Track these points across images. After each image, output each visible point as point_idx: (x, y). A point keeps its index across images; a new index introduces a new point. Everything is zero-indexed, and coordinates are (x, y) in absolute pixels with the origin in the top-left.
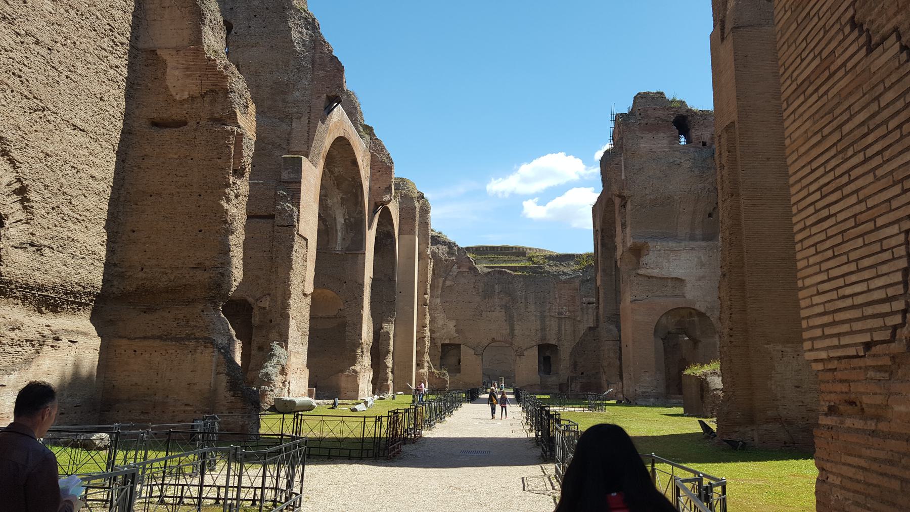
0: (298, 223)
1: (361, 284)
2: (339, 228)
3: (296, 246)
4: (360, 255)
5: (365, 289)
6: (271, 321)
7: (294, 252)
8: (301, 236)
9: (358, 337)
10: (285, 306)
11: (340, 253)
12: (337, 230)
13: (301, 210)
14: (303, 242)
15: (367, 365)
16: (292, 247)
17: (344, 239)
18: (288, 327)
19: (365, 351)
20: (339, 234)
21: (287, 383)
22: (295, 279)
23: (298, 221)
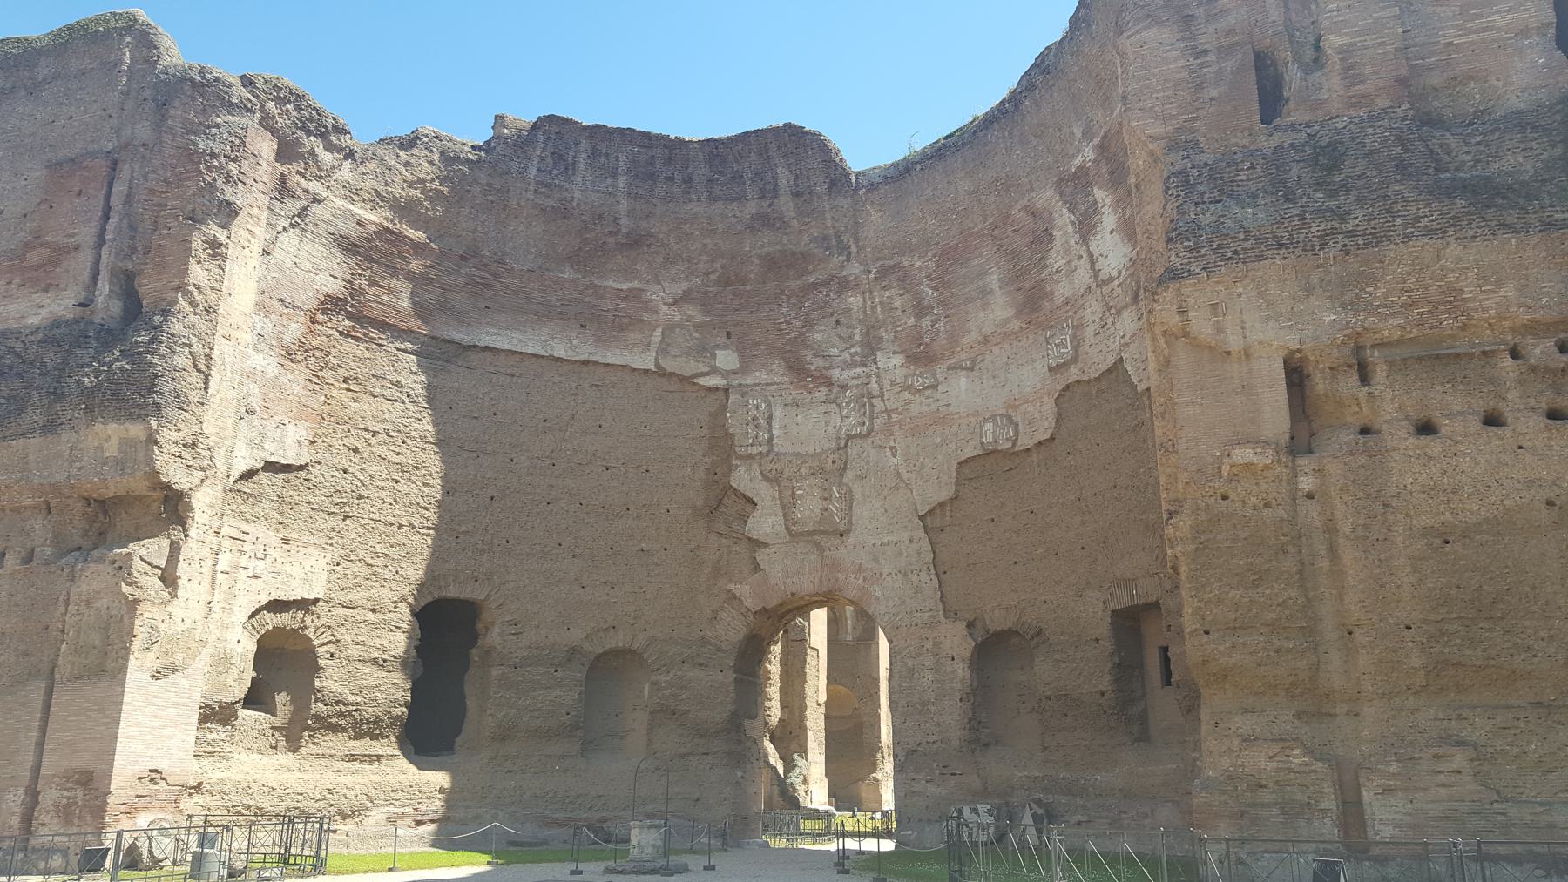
0: (809, 636)
1: (876, 679)
2: (848, 615)
3: (808, 660)
4: (873, 646)
5: (881, 684)
6: (791, 733)
7: (807, 666)
8: (812, 648)
9: (877, 740)
10: (803, 718)
11: (851, 643)
12: (846, 619)
13: (811, 624)
14: (815, 653)
15: (889, 772)
16: (805, 661)
17: (854, 628)
18: (807, 738)
19: (886, 755)
20: (849, 622)
21: (809, 792)
22: (809, 691)
23: (809, 634)
